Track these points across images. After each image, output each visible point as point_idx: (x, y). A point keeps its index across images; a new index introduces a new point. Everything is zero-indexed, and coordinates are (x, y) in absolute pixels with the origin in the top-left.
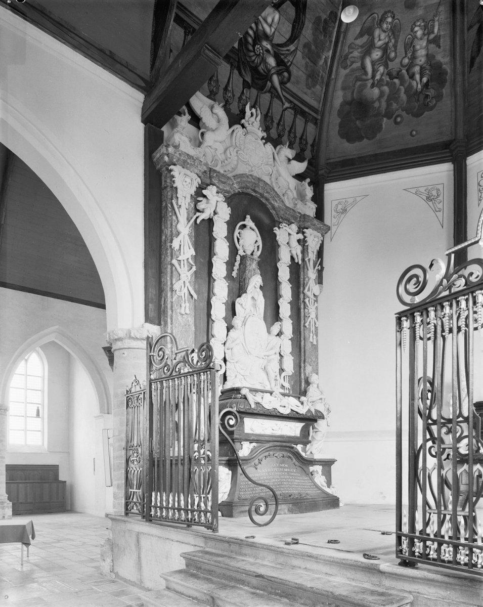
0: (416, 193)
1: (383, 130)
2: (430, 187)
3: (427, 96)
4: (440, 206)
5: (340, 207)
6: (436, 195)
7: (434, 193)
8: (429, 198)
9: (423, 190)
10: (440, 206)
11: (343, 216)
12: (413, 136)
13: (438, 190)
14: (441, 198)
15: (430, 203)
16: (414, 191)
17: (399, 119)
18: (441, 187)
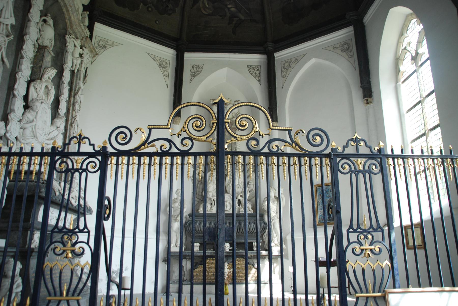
0: (153, 59)
1: (140, 9)
2: (162, 59)
3: (168, 6)
4: (167, 73)
5: (101, 43)
6: (165, 66)
7: (164, 64)
8: (161, 66)
9: (158, 59)
10: (167, 73)
11: (103, 50)
12: (157, 24)
13: (166, 63)
14: (167, 68)
15: (162, 69)
16: (153, 57)
17: (150, 9)
18: (167, 61)
